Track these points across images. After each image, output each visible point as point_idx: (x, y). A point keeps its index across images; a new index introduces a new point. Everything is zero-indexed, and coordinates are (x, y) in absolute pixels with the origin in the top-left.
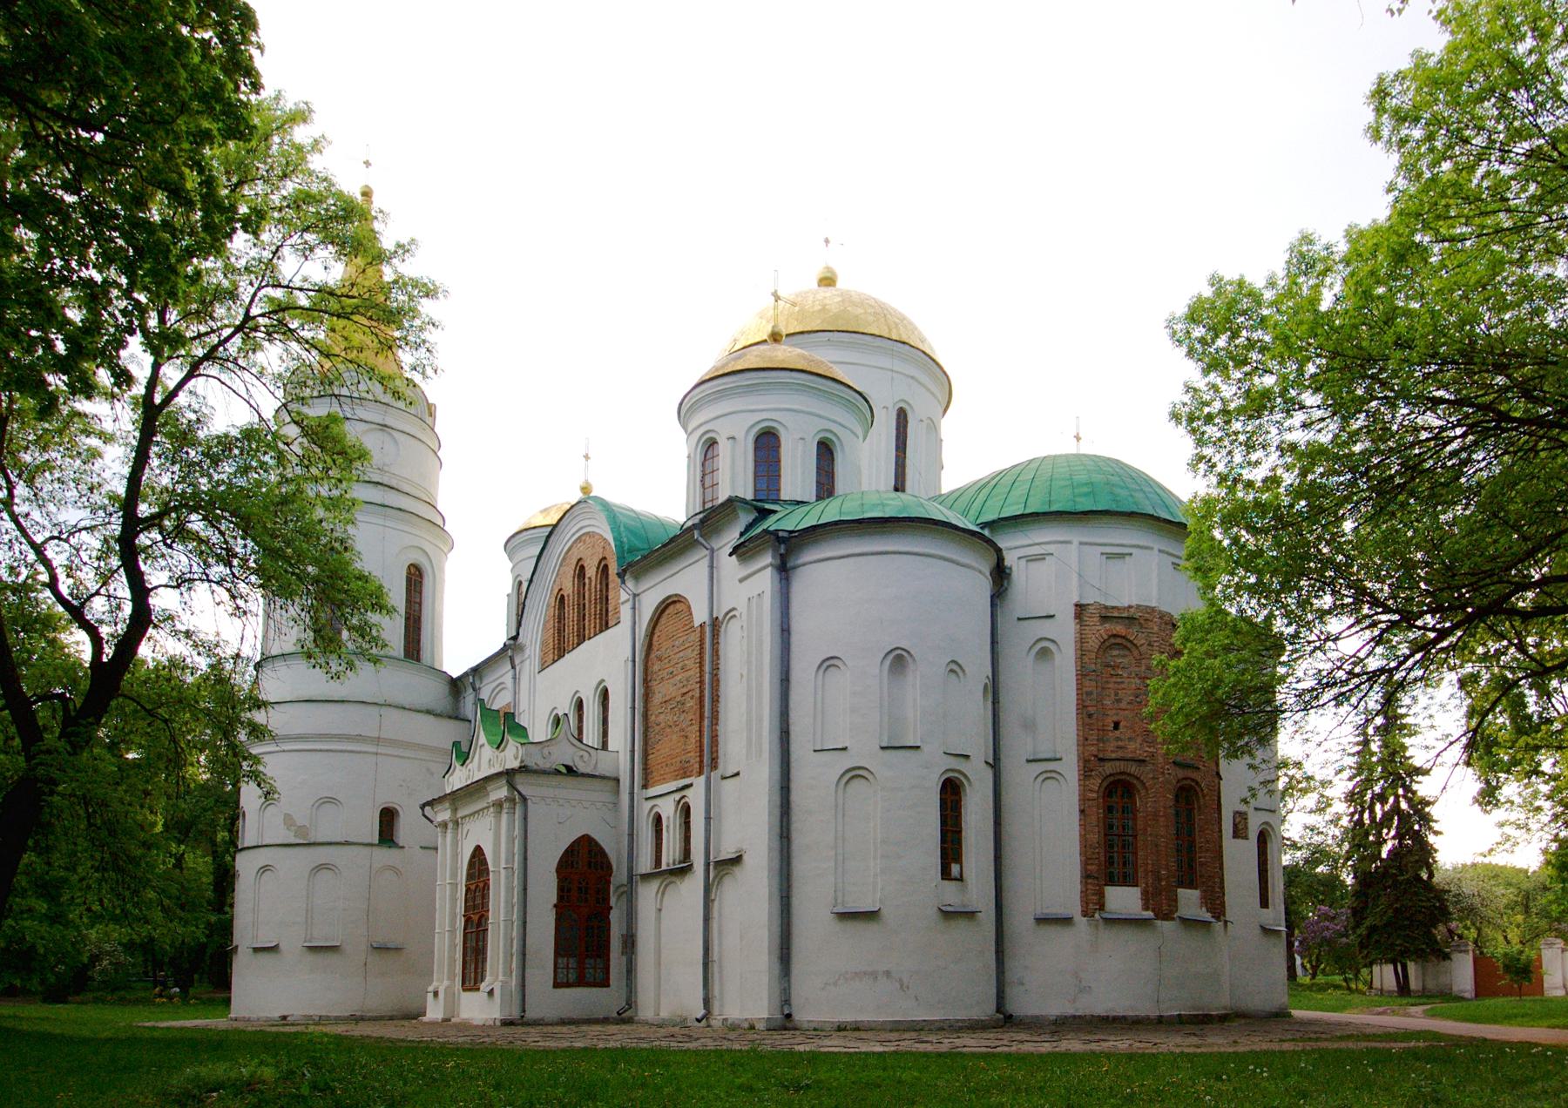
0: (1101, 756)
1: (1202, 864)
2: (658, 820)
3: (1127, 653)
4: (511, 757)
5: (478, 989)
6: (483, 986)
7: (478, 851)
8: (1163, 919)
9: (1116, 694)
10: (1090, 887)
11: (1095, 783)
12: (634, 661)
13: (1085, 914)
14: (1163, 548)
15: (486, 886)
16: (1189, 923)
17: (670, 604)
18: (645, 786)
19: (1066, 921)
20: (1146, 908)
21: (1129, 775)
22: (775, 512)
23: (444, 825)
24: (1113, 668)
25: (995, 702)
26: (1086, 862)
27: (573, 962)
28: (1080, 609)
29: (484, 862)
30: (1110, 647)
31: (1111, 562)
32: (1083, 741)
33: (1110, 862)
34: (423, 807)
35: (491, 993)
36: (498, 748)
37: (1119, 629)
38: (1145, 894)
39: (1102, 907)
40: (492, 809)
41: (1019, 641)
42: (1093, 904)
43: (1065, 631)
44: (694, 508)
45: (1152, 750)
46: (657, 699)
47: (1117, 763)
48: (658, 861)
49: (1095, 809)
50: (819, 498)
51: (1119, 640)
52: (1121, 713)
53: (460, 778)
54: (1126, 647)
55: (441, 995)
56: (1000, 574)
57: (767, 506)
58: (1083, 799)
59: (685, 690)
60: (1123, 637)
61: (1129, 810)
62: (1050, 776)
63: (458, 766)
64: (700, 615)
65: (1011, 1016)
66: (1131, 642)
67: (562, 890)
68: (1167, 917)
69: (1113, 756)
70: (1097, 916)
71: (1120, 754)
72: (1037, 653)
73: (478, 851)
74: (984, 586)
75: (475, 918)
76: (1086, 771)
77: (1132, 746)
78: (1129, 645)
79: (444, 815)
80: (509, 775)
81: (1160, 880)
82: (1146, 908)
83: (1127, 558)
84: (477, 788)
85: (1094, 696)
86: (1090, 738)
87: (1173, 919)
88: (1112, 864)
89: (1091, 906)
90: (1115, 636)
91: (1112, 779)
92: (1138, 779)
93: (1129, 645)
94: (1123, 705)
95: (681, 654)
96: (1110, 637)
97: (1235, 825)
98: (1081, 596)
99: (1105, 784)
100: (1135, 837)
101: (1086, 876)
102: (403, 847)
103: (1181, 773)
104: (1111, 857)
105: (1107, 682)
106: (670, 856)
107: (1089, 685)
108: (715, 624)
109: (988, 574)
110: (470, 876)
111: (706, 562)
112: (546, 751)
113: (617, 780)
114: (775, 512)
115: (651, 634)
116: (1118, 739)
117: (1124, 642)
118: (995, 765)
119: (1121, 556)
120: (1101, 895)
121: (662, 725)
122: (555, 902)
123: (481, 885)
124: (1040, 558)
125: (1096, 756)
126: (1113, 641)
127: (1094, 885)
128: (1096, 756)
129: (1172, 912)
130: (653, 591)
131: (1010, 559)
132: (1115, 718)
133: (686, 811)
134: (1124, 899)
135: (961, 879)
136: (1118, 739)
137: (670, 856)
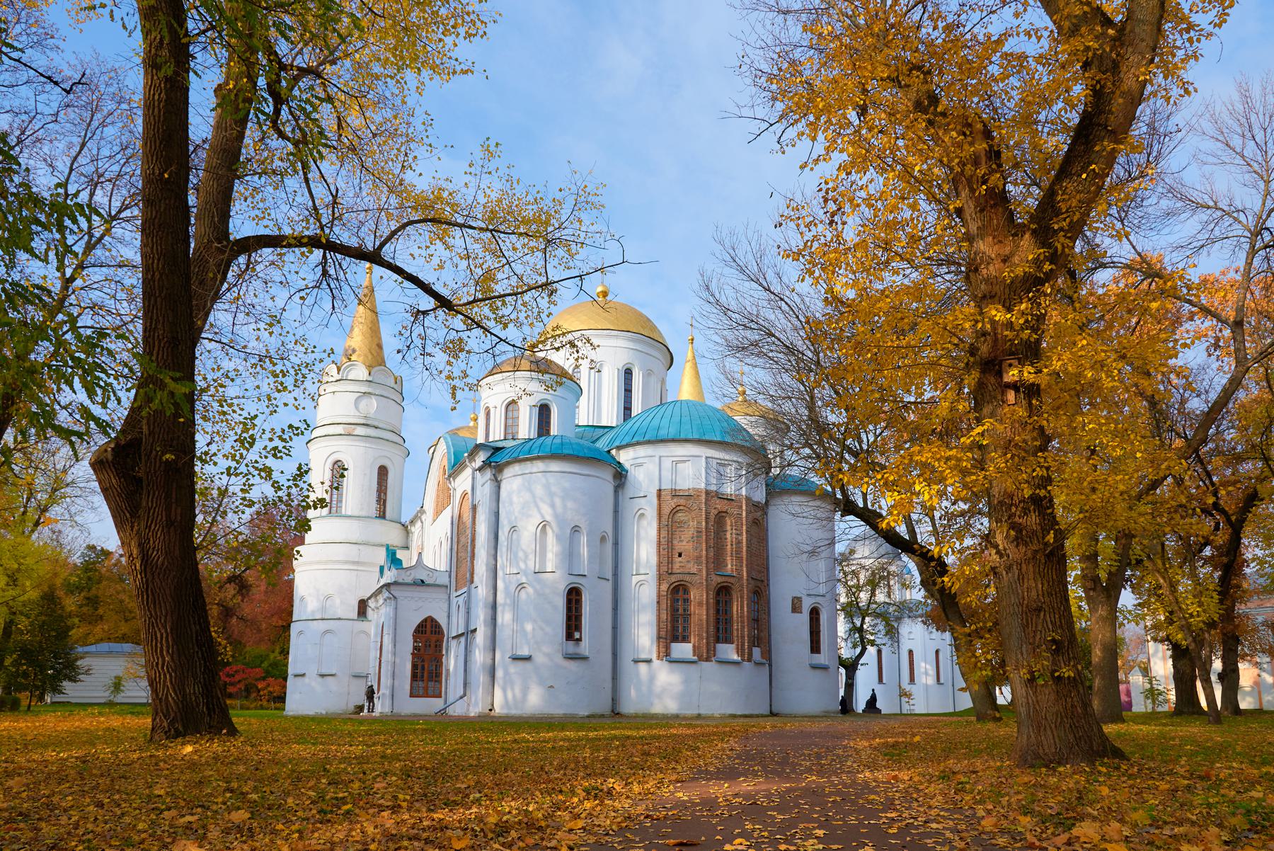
11: (664, 587)
13: (659, 658)
33: (674, 628)
37: (682, 501)
41: (630, 508)
46: (461, 543)
50: (540, 435)
58: (659, 596)
68: (708, 659)
76: (660, 579)
107: (664, 533)
112: (408, 573)
119: (685, 461)
134: (683, 650)
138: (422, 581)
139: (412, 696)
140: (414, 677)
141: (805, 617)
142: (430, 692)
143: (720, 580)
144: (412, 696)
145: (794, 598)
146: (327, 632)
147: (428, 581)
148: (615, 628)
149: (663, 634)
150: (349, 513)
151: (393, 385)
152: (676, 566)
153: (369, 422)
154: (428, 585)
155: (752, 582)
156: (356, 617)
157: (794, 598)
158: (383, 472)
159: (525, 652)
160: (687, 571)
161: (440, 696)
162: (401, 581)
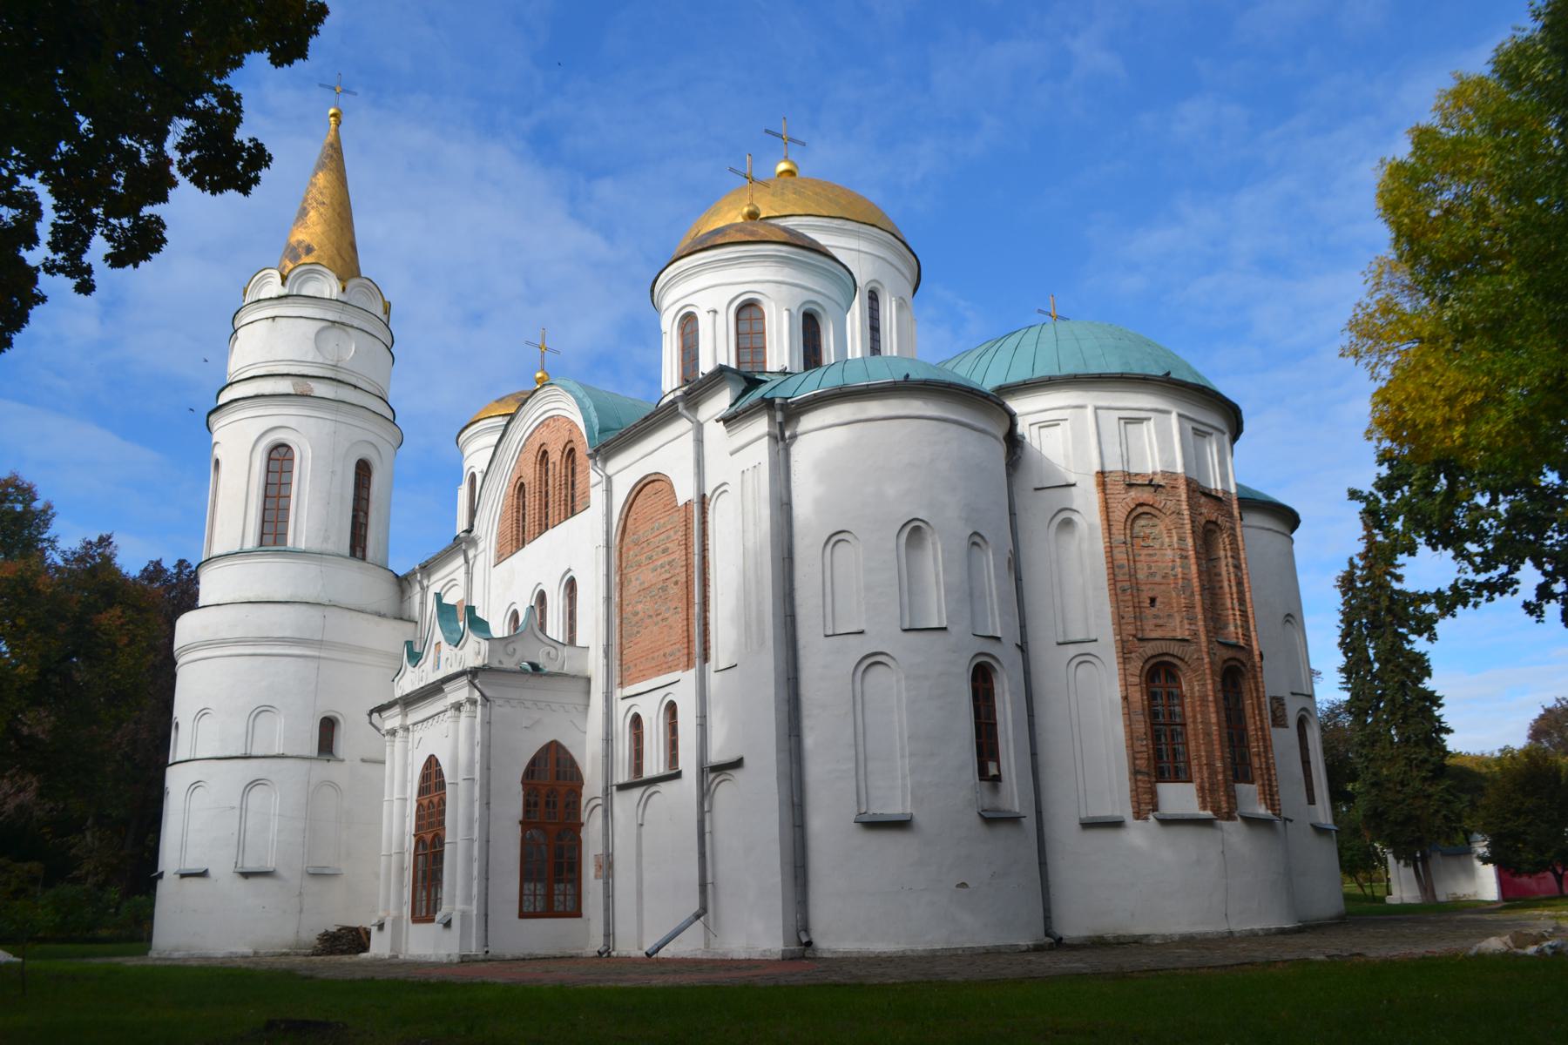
0: (1140, 636)
2: (637, 721)
3: (1156, 521)
4: (473, 652)
5: (432, 920)
6: (438, 917)
7: (432, 764)
9: (1150, 568)
10: (1140, 784)
11: (1136, 666)
12: (608, 547)
13: (1138, 815)
14: (1182, 412)
15: (443, 801)
16: (1251, 821)
17: (652, 484)
18: (621, 685)
19: (1117, 824)
20: (1204, 808)
22: (765, 382)
23: (393, 732)
25: (1018, 580)
26: (1133, 758)
27: (540, 889)
29: (440, 773)
30: (1138, 516)
32: (1119, 619)
33: (1158, 755)
34: (372, 712)
35: (448, 925)
36: (456, 646)
37: (1146, 495)
38: (1201, 789)
39: (1155, 808)
40: (449, 714)
42: (1145, 804)
43: (1087, 504)
44: (672, 384)
45: (1193, 627)
46: (633, 588)
47: (1158, 643)
48: (638, 766)
51: (1145, 509)
53: (411, 680)
55: (388, 927)
56: (1013, 442)
57: (758, 377)
59: (668, 575)
60: (1152, 506)
61: (1174, 696)
62: (1084, 659)
63: (410, 668)
64: (685, 492)
65: (1061, 939)
66: (1160, 511)
67: (528, 806)
69: (1154, 635)
70: (1151, 817)
72: (1060, 524)
73: (432, 764)
74: (1000, 450)
75: (429, 837)
76: (1125, 655)
78: (1156, 513)
79: (392, 720)
80: (474, 673)
82: (1204, 808)
83: (1145, 423)
84: (433, 690)
85: (1126, 570)
87: (1234, 819)
88: (1160, 757)
89: (1143, 807)
90: (1141, 505)
91: (1154, 661)
92: (1182, 659)
93: (1156, 513)
95: (662, 537)
97: (1273, 712)
98: (1102, 464)
99: (1147, 667)
100: (1184, 725)
101: (1135, 772)
102: (343, 760)
103: (1227, 654)
104: (1160, 750)
105: (1140, 555)
106: (654, 764)
108: (703, 501)
109: (1001, 438)
110: (422, 791)
111: (688, 442)
112: (510, 648)
113: (588, 680)
114: (765, 382)
115: (630, 504)
116: (1156, 617)
118: (1023, 648)
119: (1140, 421)
120: (1153, 794)
121: (641, 615)
122: (521, 818)
123: (436, 800)
124: (1054, 424)
125: (1134, 636)
126: (1140, 510)
127: (1144, 782)
128: (1134, 636)
130: (628, 468)
131: (1022, 427)
132: (1151, 594)
133: (672, 708)
134: (1180, 798)
135: (997, 779)
136: (1156, 617)
137: (654, 764)
138: (535, 667)
139: (523, 915)
140: (527, 875)
141: (1291, 733)
142: (559, 908)
144: (523, 915)
146: (255, 783)
147: (549, 667)
148: (1034, 754)
149: (1142, 764)
150: (302, 546)
151: (380, 314)
152: (1149, 625)
153: (340, 377)
154: (551, 675)
156: (315, 753)
158: (363, 471)
159: (895, 808)
160: (1170, 635)
161: (577, 913)
162: (495, 664)
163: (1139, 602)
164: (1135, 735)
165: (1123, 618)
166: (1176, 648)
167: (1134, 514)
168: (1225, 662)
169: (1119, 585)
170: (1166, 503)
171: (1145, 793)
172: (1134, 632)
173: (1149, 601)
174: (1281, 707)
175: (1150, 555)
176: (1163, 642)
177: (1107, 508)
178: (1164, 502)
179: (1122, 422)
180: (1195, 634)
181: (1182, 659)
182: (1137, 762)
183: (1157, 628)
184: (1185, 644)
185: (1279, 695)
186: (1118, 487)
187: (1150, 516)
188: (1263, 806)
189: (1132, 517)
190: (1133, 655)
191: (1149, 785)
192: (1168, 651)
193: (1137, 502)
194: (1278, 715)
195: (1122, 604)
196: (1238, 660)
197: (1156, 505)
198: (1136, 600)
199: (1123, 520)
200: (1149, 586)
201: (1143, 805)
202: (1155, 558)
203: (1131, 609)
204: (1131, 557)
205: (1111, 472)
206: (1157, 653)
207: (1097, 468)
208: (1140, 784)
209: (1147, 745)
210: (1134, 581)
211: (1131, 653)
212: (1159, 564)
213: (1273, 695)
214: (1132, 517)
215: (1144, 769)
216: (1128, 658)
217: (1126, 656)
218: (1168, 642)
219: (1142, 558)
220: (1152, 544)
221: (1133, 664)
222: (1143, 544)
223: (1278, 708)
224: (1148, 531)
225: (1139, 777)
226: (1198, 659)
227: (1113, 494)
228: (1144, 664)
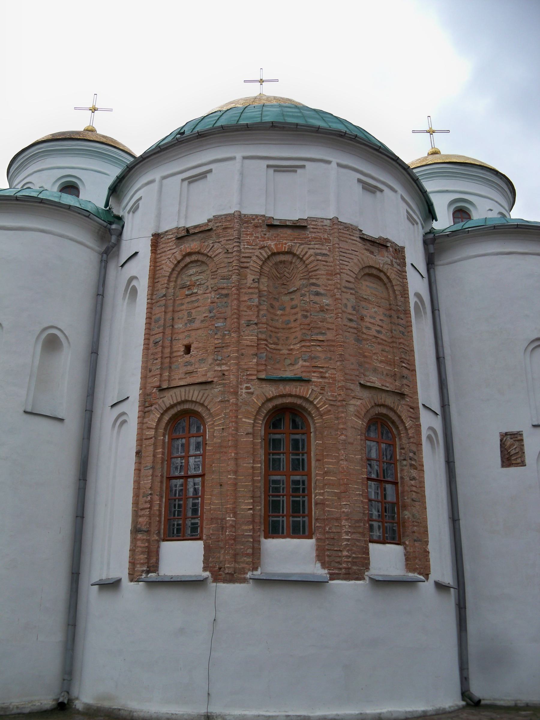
1: (321, 504)
3: (204, 268)
8: (225, 581)
9: (189, 314)
10: (139, 543)
11: (153, 419)
13: (133, 577)
21: (192, 402)
24: (189, 287)
26: (136, 515)
28: (157, 238)
31: (194, 185)
37: (193, 245)
38: (208, 549)
39: (153, 567)
49: (151, 448)
51: (194, 258)
52: (193, 333)
54: (203, 262)
58: (140, 440)
60: (199, 253)
71: (189, 380)
77: (203, 368)
78: (204, 259)
81: (223, 529)
82: (205, 569)
83: (209, 175)
86: (154, 368)
87: (244, 581)
89: (138, 568)
90: (189, 254)
92: (202, 405)
93: (204, 259)
94: (197, 324)
96: (184, 256)
99: (166, 418)
101: (136, 530)
107: (158, 311)
117: (200, 258)
119: (203, 176)
126: (188, 260)
129: (243, 571)
132: (186, 342)
143: (271, 390)
145: (504, 436)
155: (366, 394)
157: (504, 436)
163: (171, 353)
164: (142, 491)
165: (150, 371)
166: (196, 393)
167: (182, 265)
168: (269, 400)
169: (152, 339)
170: (213, 246)
171: (143, 553)
172: (157, 384)
173: (183, 349)
174: (517, 444)
175: (192, 302)
176: (183, 389)
177: (155, 267)
178: (211, 245)
179: (186, 183)
180: (224, 375)
181: (202, 405)
182: (140, 520)
183: (187, 375)
184: (208, 387)
185: (515, 429)
186: (171, 244)
187: (199, 263)
188: (319, 565)
189: (178, 269)
190: (153, 408)
191: (147, 544)
192: (187, 398)
193: (184, 253)
194: (513, 452)
195: (152, 357)
196: (296, 396)
197: (202, 251)
198: (167, 350)
199: (168, 274)
200: (186, 334)
201: (138, 566)
202: (196, 304)
203: (159, 360)
204: (171, 309)
205: (167, 232)
206: (175, 402)
207: (153, 232)
208: (139, 543)
209: (151, 502)
210: (168, 331)
211: (151, 406)
212: (199, 309)
213: (504, 430)
214: (178, 269)
215: (144, 528)
216: (148, 411)
217: (147, 409)
218: (187, 388)
219: (184, 307)
220: (195, 291)
221: (152, 416)
222: (187, 293)
223: (512, 445)
224: (194, 278)
225: (140, 536)
226: (221, 401)
227: (165, 252)
228: (162, 414)
